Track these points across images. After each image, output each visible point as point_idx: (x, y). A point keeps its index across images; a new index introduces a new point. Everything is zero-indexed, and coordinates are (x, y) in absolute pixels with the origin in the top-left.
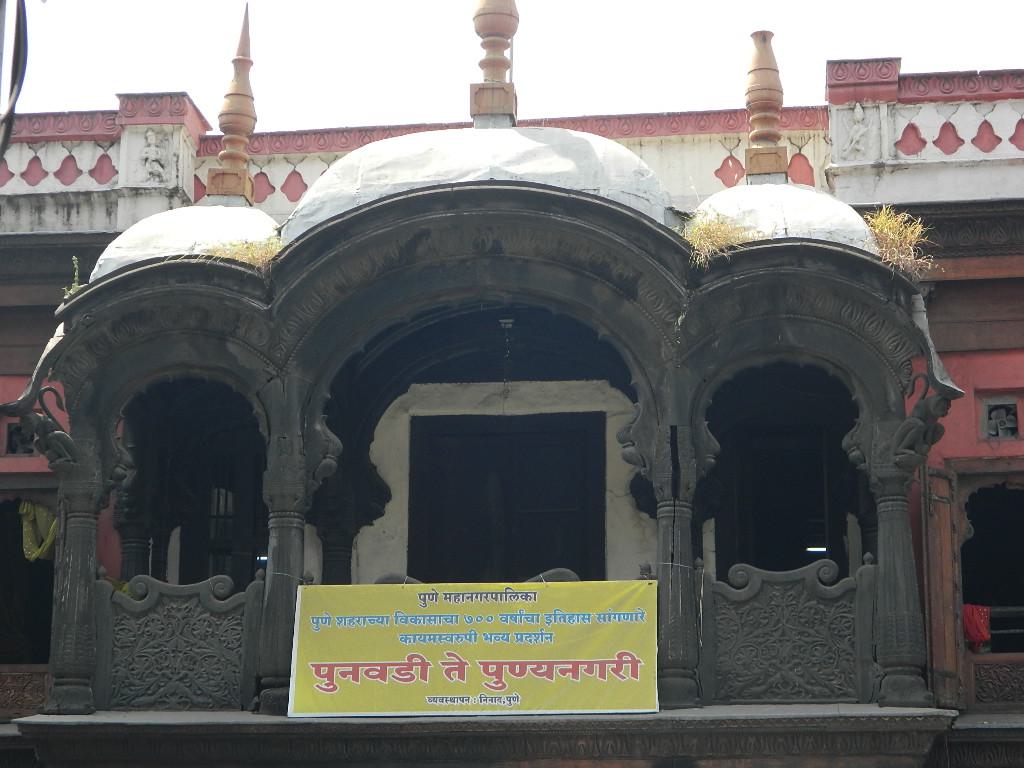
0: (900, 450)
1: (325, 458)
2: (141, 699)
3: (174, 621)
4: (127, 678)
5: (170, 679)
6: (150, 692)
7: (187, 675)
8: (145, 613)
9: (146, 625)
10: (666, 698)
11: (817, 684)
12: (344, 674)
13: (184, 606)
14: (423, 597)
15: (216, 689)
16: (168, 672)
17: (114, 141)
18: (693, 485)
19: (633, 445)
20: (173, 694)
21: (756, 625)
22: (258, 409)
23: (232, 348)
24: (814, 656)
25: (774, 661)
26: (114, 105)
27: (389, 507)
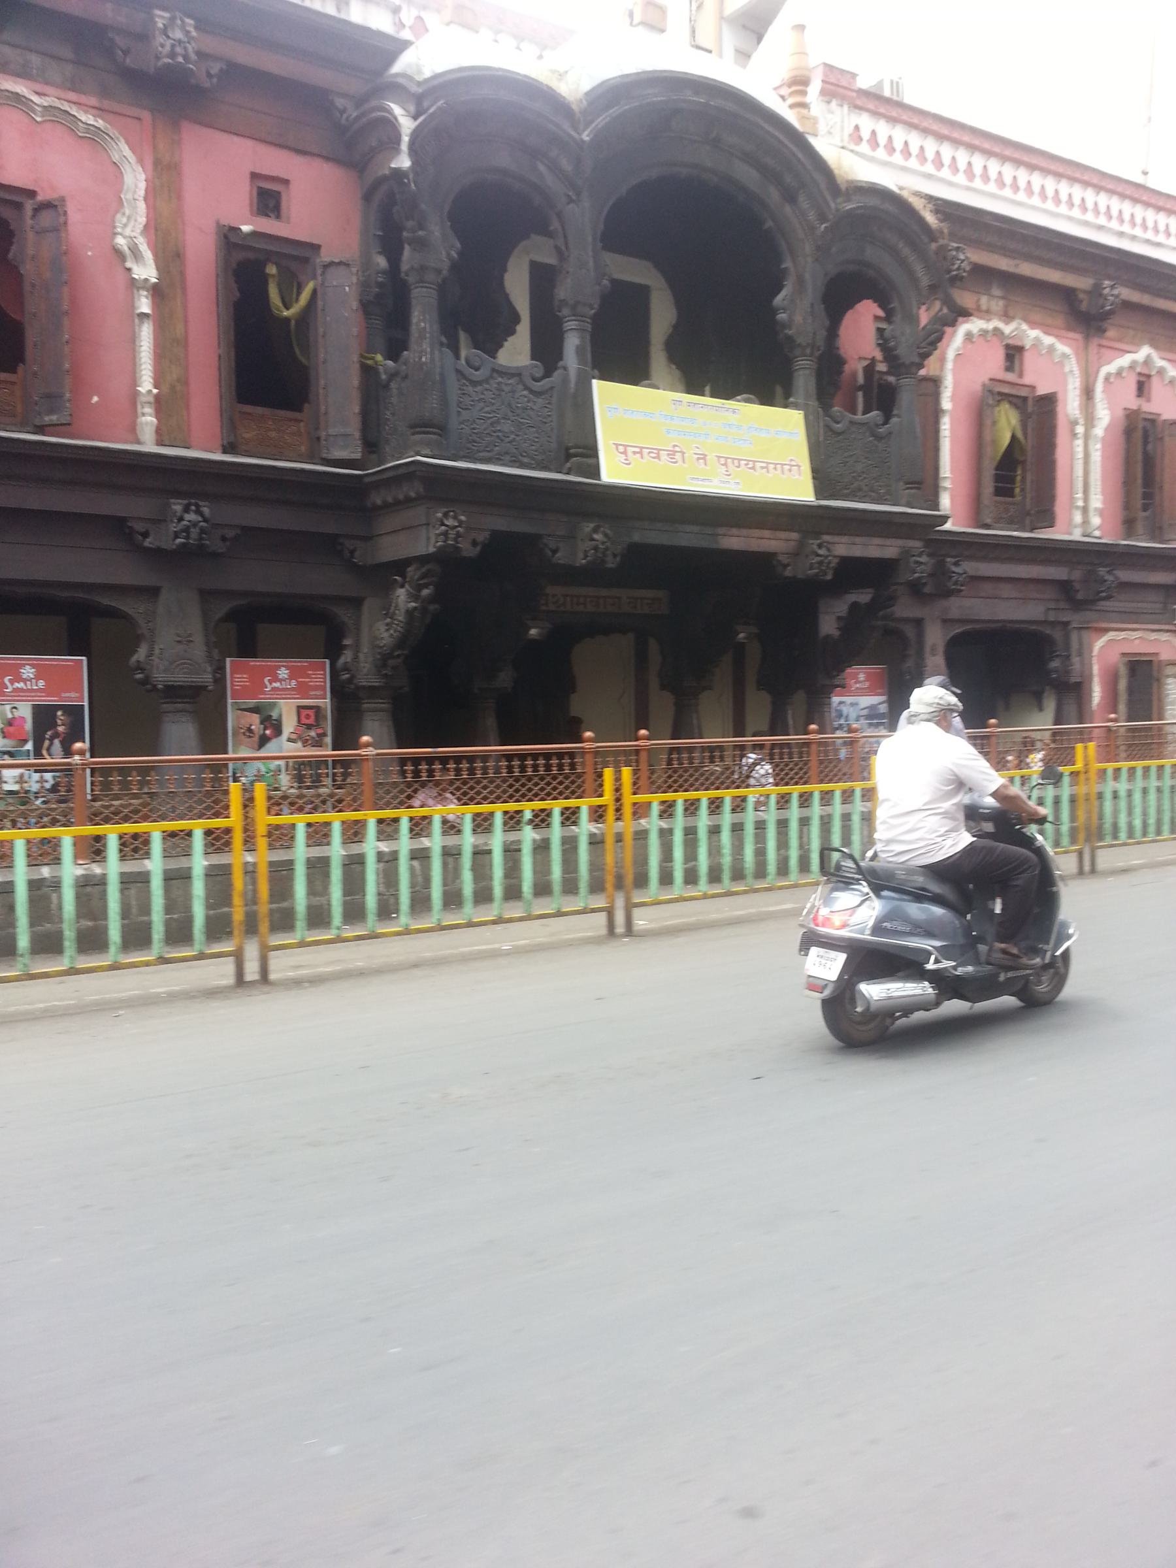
0: (923, 345)
2: (481, 454)
3: (503, 393)
4: (470, 436)
5: (502, 440)
6: (488, 449)
10: (820, 492)
12: (634, 453)
14: (689, 404)
20: (507, 453)
23: (542, 168)
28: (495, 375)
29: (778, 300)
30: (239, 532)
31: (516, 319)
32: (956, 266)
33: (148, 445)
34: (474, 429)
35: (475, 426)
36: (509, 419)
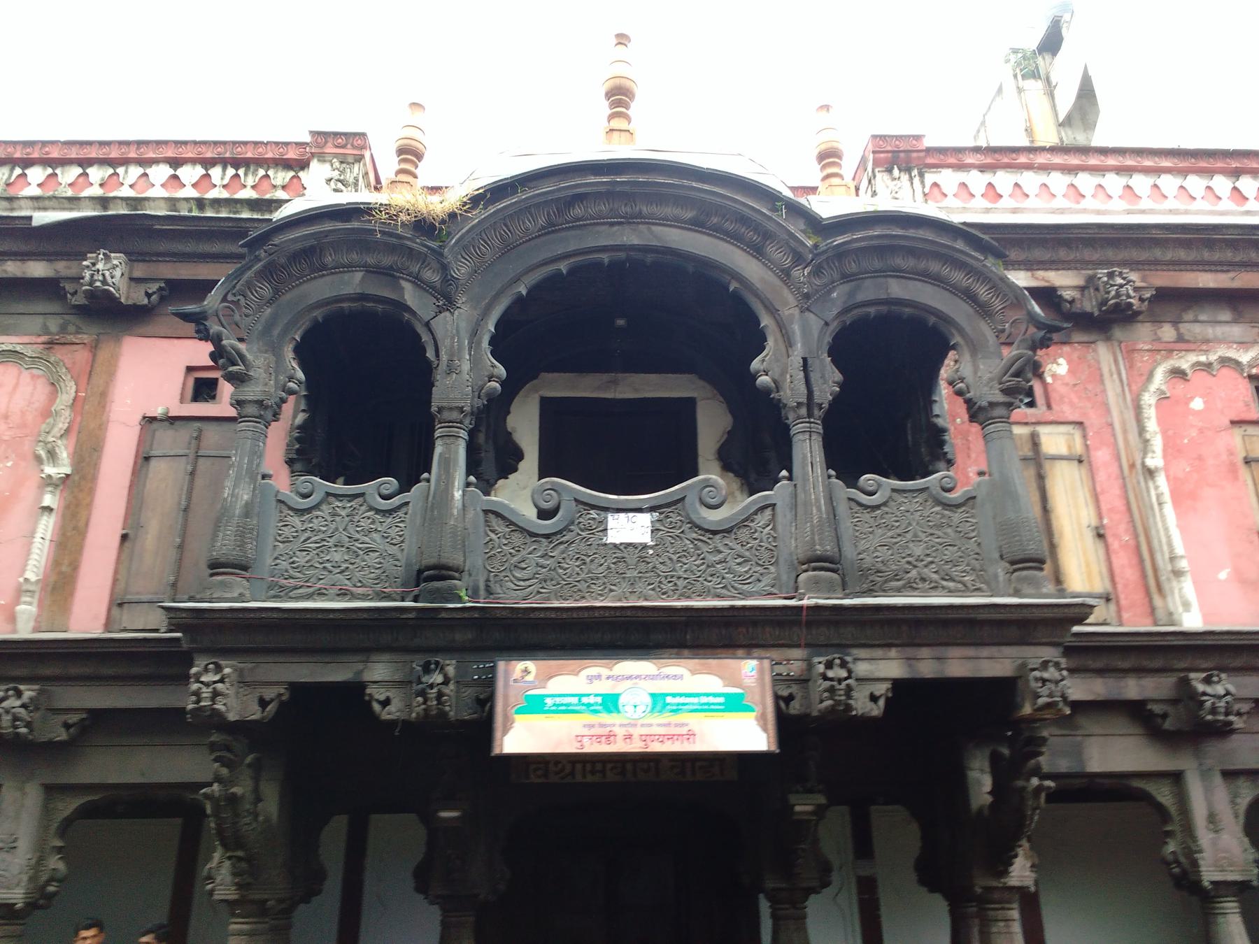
1: (490, 381)
3: (338, 519)
4: (287, 571)
5: (331, 572)
7: (347, 568)
8: (309, 510)
9: (311, 522)
11: (952, 580)
13: (349, 505)
15: (376, 582)
16: (328, 565)
17: (303, 165)
18: (826, 405)
19: (767, 375)
21: (889, 527)
22: (425, 337)
24: (945, 555)
25: (910, 559)
26: (308, 139)
27: (522, 465)
28: (331, 499)
29: (756, 364)
30: (84, 716)
31: (519, 455)
32: (1113, 293)
33: (24, 631)
34: (293, 563)
35: (295, 559)
36: (342, 546)
